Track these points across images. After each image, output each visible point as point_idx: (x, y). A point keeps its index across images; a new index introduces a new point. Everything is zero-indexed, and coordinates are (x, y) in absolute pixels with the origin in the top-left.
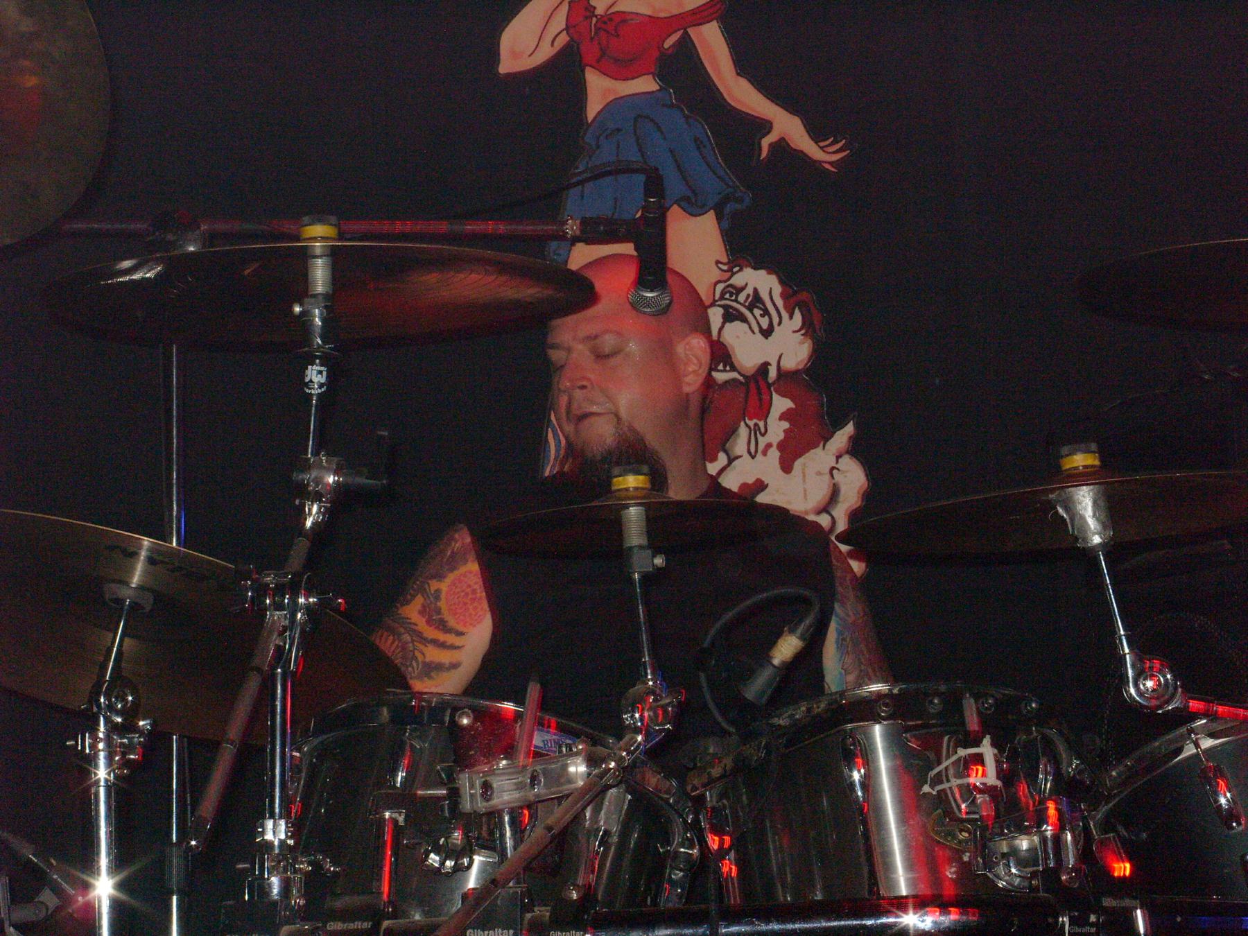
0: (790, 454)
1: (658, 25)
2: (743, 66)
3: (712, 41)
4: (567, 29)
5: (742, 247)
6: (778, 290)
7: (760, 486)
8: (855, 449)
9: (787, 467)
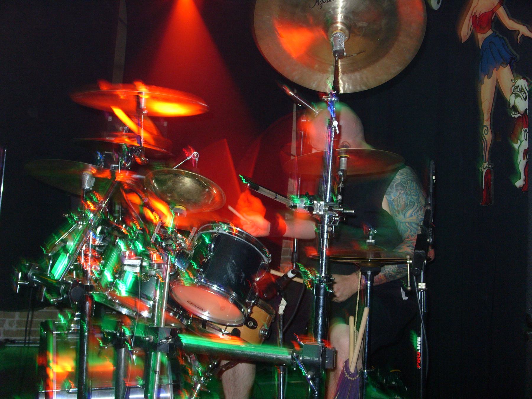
3: (502, 12)
6: (526, 84)
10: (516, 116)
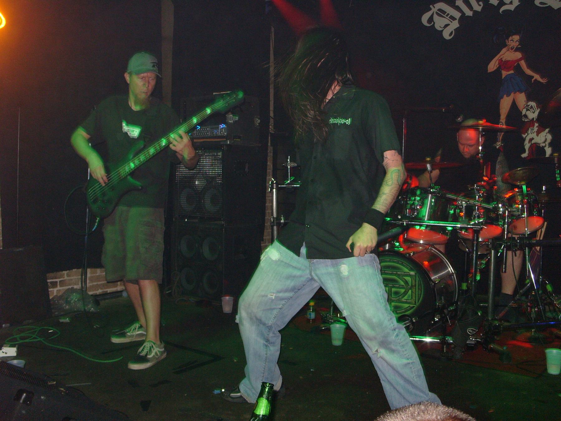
0: (538, 133)
1: (514, 62)
2: (529, 67)
3: (523, 63)
4: (499, 64)
5: (529, 99)
7: (533, 139)
8: (549, 132)
9: (537, 135)
10: (526, 120)
